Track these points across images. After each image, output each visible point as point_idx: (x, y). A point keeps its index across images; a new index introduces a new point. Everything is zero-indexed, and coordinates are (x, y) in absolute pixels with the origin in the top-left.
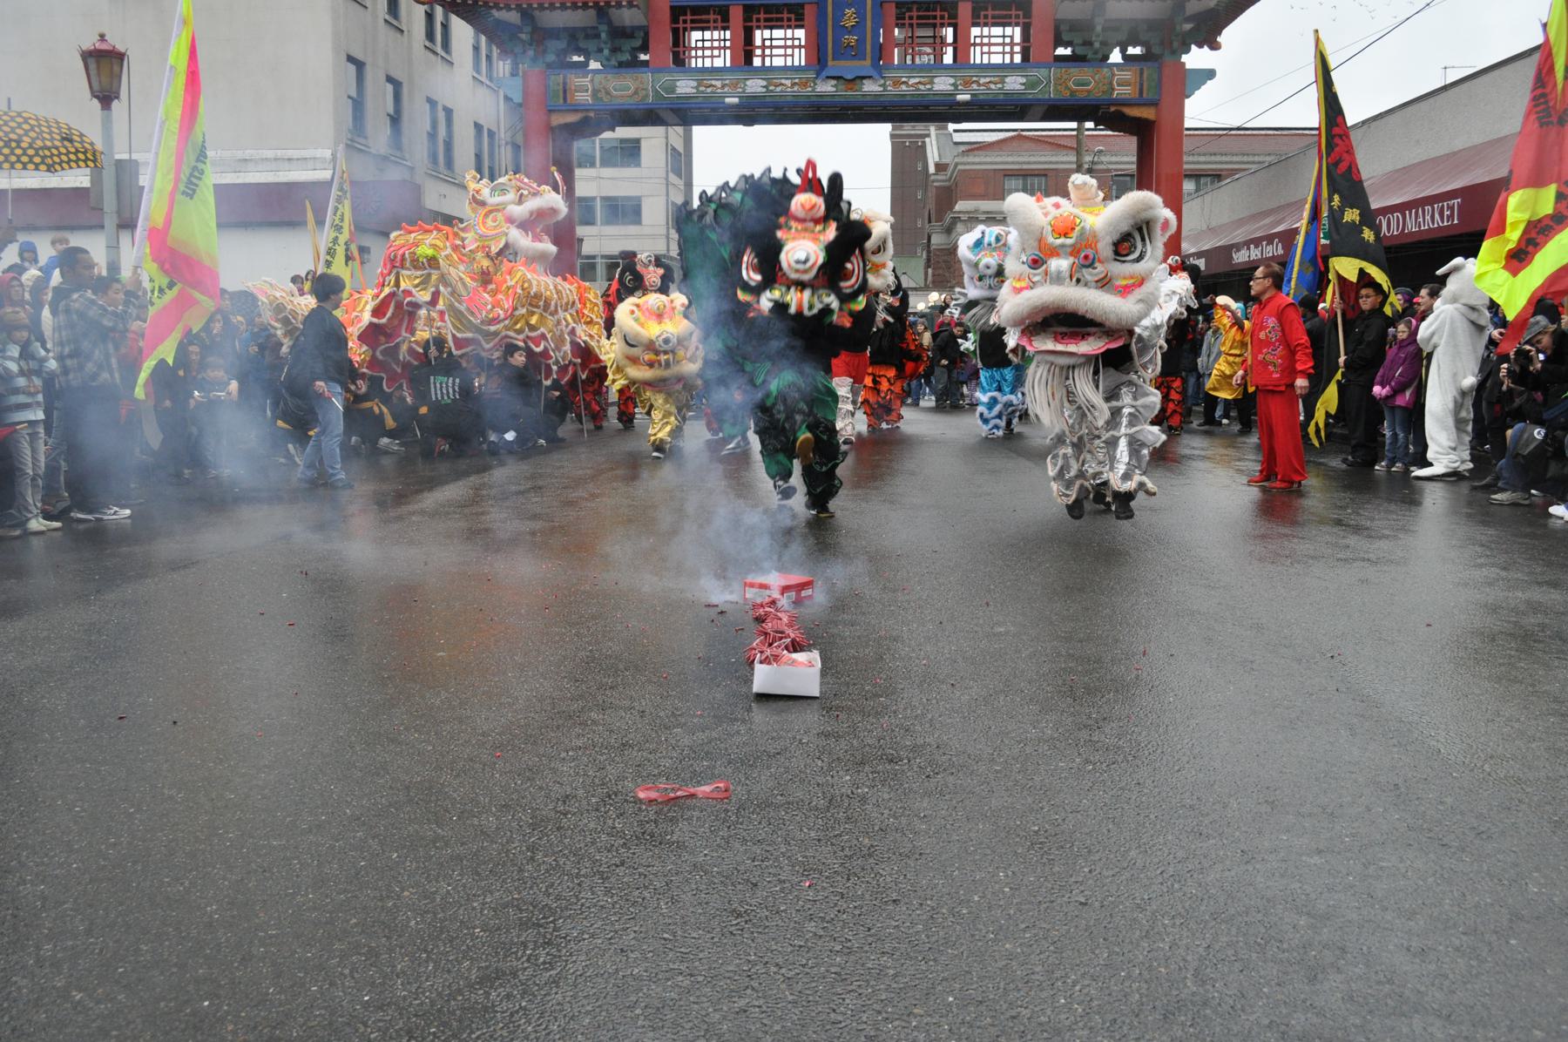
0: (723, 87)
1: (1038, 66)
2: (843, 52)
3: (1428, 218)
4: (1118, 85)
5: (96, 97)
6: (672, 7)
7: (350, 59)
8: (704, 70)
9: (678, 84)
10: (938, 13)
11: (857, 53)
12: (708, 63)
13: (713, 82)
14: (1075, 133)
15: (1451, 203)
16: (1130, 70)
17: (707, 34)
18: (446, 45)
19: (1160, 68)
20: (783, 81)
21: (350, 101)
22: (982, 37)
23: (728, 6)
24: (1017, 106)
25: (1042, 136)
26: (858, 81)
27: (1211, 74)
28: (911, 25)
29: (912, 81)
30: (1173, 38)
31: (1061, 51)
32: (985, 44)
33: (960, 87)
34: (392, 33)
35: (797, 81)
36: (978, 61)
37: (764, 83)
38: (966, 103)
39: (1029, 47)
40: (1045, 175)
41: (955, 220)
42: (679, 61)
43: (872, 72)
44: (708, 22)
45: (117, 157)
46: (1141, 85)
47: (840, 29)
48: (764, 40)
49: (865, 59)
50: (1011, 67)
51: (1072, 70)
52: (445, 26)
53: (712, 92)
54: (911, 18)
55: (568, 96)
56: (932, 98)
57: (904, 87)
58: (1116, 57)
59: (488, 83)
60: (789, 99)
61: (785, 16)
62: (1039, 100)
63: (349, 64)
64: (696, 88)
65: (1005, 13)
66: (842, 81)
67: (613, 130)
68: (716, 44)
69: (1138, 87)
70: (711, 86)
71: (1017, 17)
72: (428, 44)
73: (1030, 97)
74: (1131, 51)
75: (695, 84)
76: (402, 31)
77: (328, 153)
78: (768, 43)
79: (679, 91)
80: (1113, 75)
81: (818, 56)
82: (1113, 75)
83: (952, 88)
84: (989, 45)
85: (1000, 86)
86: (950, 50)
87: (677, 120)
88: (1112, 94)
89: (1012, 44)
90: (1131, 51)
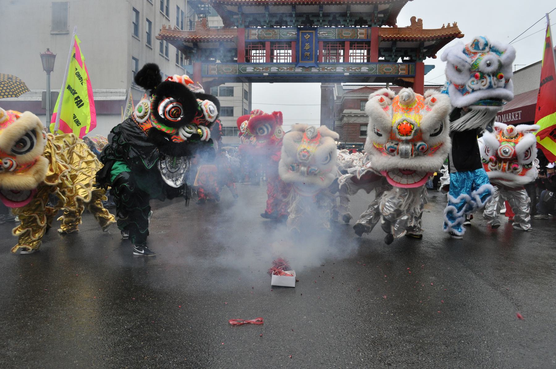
0: (263, 69)
1: (373, 63)
2: (304, 58)
3: (510, 117)
4: (401, 70)
5: (45, 70)
6: (245, 42)
7: (134, 58)
8: (256, 63)
9: (247, 68)
10: (338, 45)
11: (310, 58)
12: (258, 61)
13: (260, 68)
14: (386, 86)
15: (518, 112)
16: (405, 65)
17: (258, 51)
18: (167, 54)
19: (415, 65)
20: (284, 68)
21: (133, 25)
22: (353, 53)
23: (265, 42)
24: (365, 77)
25: (374, 87)
26: (310, 68)
27: (433, 67)
28: (329, 49)
29: (329, 68)
30: (420, 54)
31: (381, 58)
32: (354, 56)
34: (148, 49)
35: (289, 68)
36: (352, 62)
37: (277, 68)
38: (348, 76)
39: (370, 57)
41: (343, 116)
42: (248, 60)
43: (315, 65)
44: (258, 47)
45: (52, 91)
46: (409, 71)
47: (304, 51)
49: (312, 60)
50: (363, 64)
51: (384, 65)
52: (167, 48)
53: (259, 71)
55: (209, 71)
56: (336, 74)
57: (326, 70)
58: (400, 60)
59: (181, 67)
60: (286, 74)
62: (373, 75)
63: (133, 60)
64: (253, 70)
65: (362, 45)
66: (304, 68)
67: (224, 84)
68: (261, 55)
69: (408, 71)
70: (259, 69)
71: (366, 47)
72: (160, 53)
73: (370, 74)
74: (405, 58)
75: (253, 68)
76: (152, 49)
77: (125, 90)
79: (247, 71)
80: (399, 67)
81: (296, 60)
82: (399, 67)
83: (343, 71)
84: (356, 56)
86: (342, 58)
87: (247, 81)
88: (399, 73)
90: (405, 58)
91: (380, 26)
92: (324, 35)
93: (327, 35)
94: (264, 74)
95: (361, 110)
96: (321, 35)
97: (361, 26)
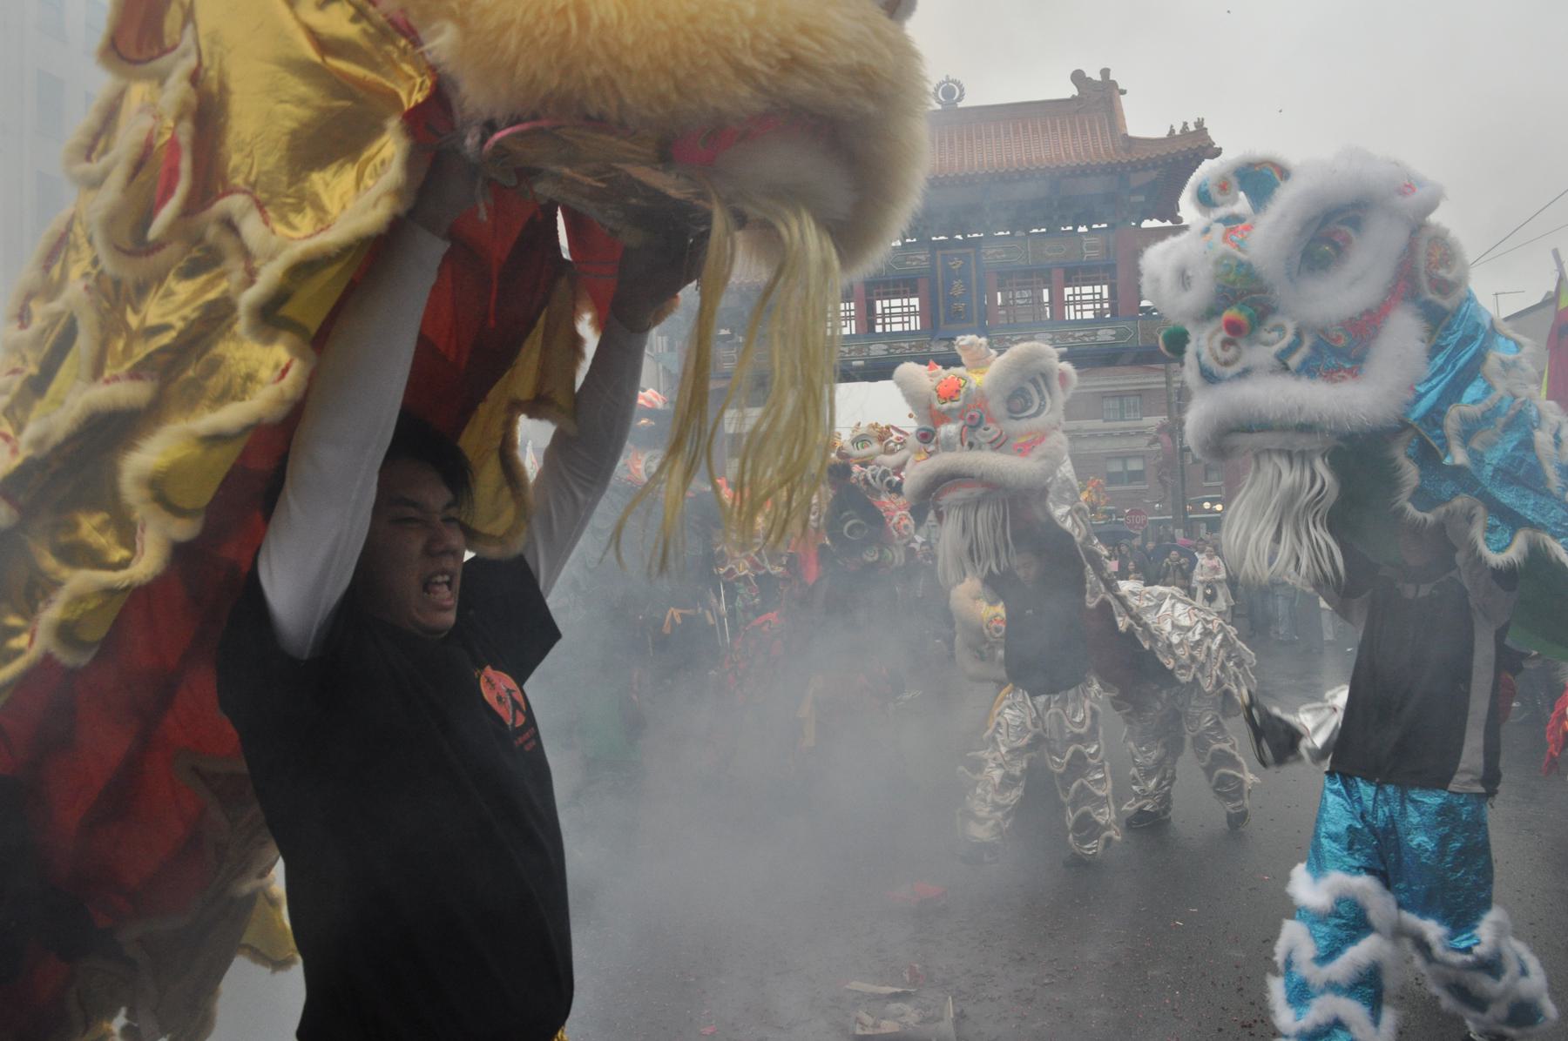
0: (850, 352)
20: (902, 344)
22: (1074, 295)
33: (1058, 341)
35: (914, 343)
36: (1072, 318)
37: (885, 347)
40: (1140, 395)
48: (883, 309)
54: (1011, 285)
61: (902, 289)
71: (1104, 278)
73: (1121, 346)
78: (887, 311)
85: (1092, 338)
86: (1048, 309)
89: (1101, 301)
91: (1139, 223)
92: (998, 257)
93: (1004, 256)
94: (854, 363)
95: (1105, 421)
96: (989, 258)
97: (1089, 227)
